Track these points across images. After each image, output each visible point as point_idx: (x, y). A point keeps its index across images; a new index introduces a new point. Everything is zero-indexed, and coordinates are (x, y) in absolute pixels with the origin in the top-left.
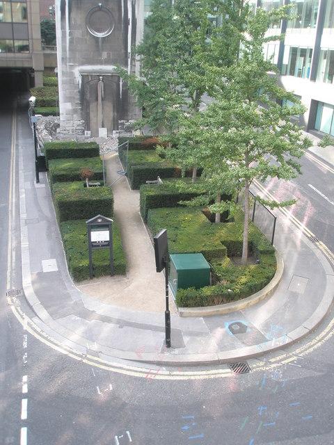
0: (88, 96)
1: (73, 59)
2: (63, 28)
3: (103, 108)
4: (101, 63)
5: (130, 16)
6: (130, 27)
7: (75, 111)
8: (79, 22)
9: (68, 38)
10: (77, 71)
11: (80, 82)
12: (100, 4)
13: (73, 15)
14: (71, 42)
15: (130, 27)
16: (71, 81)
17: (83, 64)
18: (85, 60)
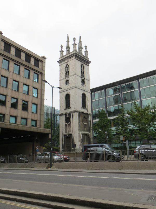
1: (80, 130)
4: (85, 131)
5: (90, 120)
7: (81, 145)
14: (80, 125)
17: (82, 131)
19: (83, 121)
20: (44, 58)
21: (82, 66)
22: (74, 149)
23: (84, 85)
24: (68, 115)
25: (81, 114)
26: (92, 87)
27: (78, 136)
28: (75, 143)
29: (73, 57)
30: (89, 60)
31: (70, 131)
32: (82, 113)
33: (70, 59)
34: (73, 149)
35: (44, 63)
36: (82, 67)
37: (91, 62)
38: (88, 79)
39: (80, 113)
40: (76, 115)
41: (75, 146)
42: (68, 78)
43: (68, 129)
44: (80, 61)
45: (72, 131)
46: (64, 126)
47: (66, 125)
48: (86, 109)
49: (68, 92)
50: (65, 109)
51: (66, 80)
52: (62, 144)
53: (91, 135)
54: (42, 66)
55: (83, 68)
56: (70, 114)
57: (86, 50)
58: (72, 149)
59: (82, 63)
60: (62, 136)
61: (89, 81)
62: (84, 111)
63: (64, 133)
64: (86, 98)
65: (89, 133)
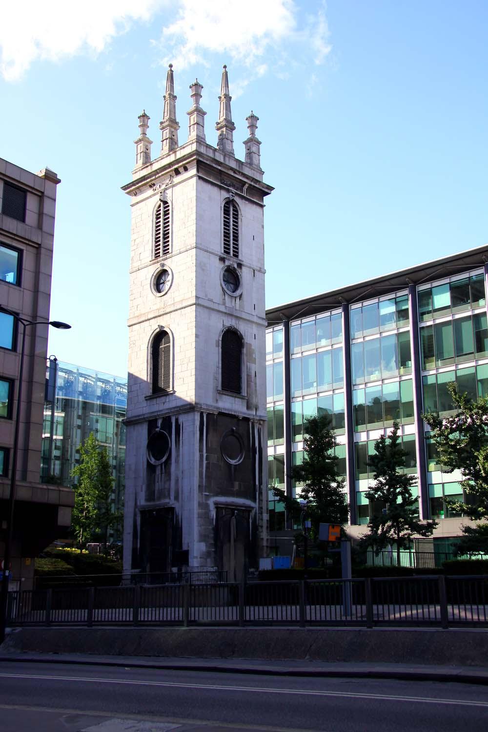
3: (235, 553)
6: (257, 456)
7: (208, 554)
9: (205, 462)
10: (211, 501)
14: (207, 468)
15: (257, 456)
16: (205, 516)
17: (217, 495)
19: (225, 449)
20: (51, 178)
21: (230, 209)
22: (180, 570)
23: (235, 294)
24: (160, 422)
26: (274, 300)
27: (196, 516)
28: (185, 548)
29: (186, 169)
30: (266, 180)
31: (167, 493)
32: (221, 414)
33: (177, 179)
34: (175, 570)
35: (47, 202)
36: (226, 212)
37: (272, 189)
38: (255, 265)
39: (208, 415)
40: (191, 425)
41: (183, 557)
42: (165, 262)
43: (158, 486)
44: (221, 188)
45: (172, 497)
46: (143, 466)
47: (151, 468)
48: (243, 398)
49: (164, 322)
50: (149, 398)
51: (155, 269)
52: (134, 550)
53: (261, 513)
54: (41, 214)
55: (236, 216)
56: (169, 418)
57: (253, 134)
58: (173, 574)
59: (225, 195)
60: (135, 515)
61: (262, 271)
62: (230, 404)
63: (142, 502)
64: (245, 350)
65: (252, 504)
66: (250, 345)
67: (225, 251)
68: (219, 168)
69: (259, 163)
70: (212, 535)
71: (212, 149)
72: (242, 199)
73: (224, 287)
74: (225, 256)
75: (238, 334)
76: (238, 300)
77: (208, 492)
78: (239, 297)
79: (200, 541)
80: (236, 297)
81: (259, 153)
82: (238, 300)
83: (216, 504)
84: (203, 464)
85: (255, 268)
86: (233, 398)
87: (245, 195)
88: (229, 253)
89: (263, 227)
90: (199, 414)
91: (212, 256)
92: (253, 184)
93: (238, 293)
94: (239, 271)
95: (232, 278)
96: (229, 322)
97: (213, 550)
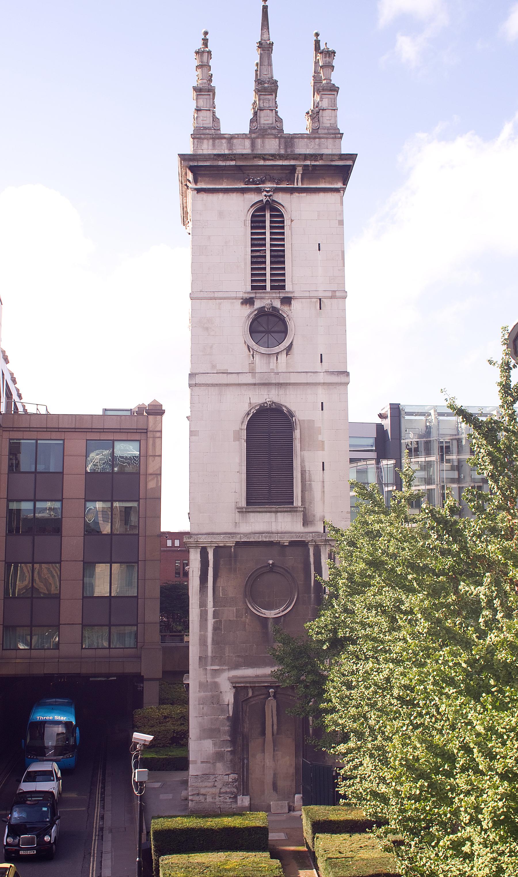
0: (247, 725)
1: (219, 657)
2: (203, 604)
7: (219, 756)
8: (231, 593)
9: (211, 622)
11: (232, 700)
12: (271, 562)
13: (221, 582)
14: (216, 629)
16: (214, 699)
17: (237, 666)
18: (240, 659)
21: (267, 220)
23: (276, 349)
25: (227, 555)
36: (257, 222)
37: (353, 157)
38: (322, 287)
39: (217, 549)
48: (294, 510)
59: (255, 198)
61: (339, 295)
62: (279, 525)
64: (297, 434)
66: (311, 422)
67: (253, 288)
68: (233, 163)
69: (336, 122)
70: (227, 728)
71: (225, 138)
72: (291, 193)
73: (252, 343)
74: (253, 295)
75: (282, 411)
76: (283, 357)
77: (218, 665)
78: (285, 352)
79: (200, 738)
80: (278, 353)
81: (335, 104)
82: (283, 357)
83: (229, 679)
84: (206, 625)
85: (321, 294)
86: (273, 514)
87: (300, 185)
88: (264, 288)
89: (341, 223)
90: (199, 550)
91: (226, 304)
92: (308, 163)
93: (286, 344)
94: (286, 308)
95: (268, 327)
96: (261, 397)
97: (229, 749)
